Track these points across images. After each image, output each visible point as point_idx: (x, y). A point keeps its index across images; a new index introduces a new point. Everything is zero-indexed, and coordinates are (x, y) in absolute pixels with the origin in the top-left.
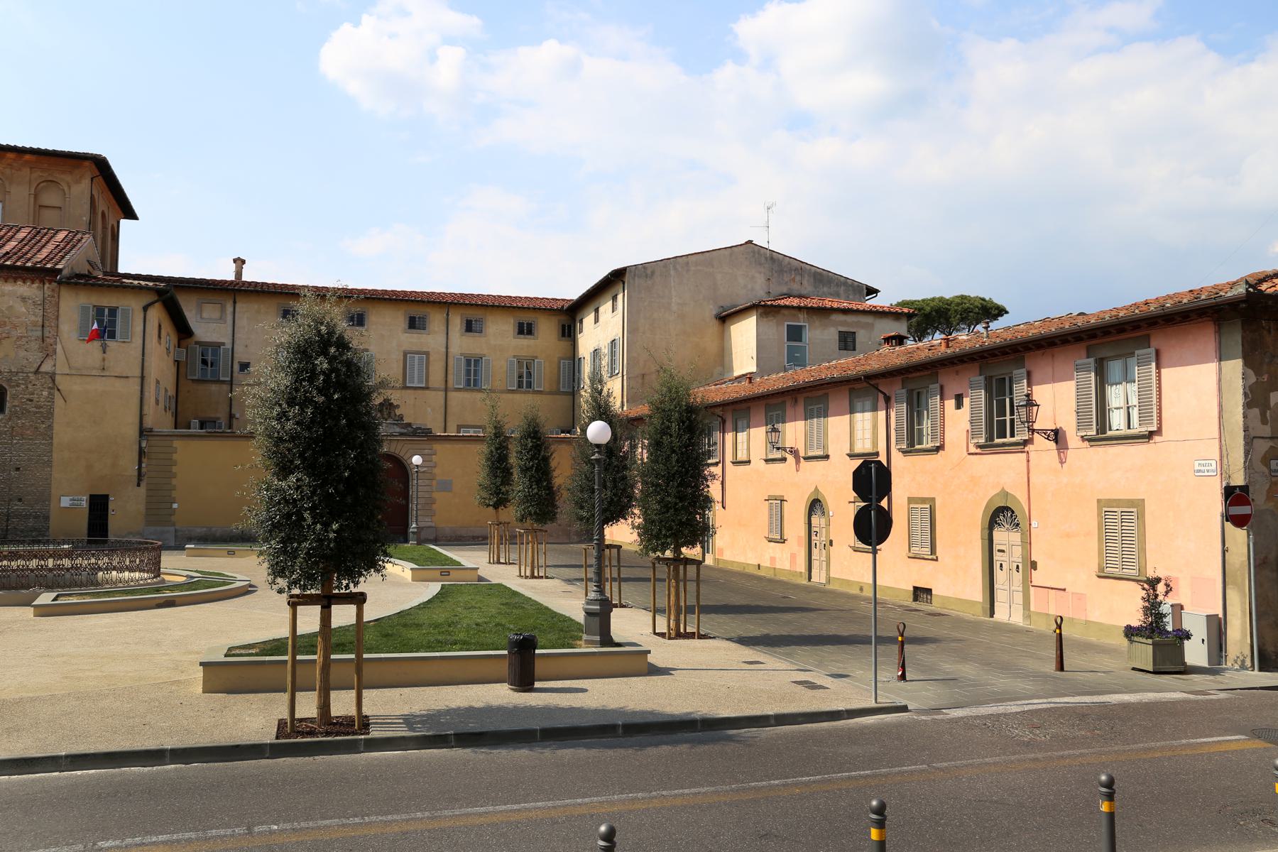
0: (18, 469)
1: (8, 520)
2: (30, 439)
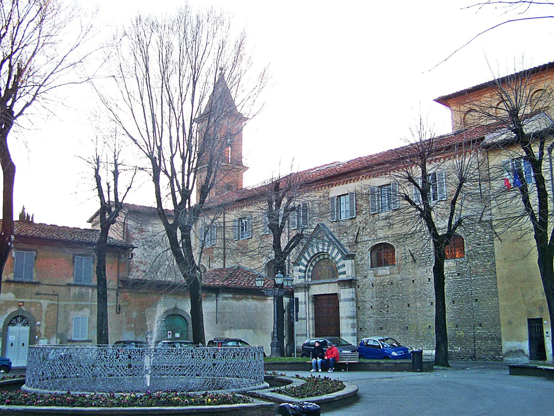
0: (477, 300)
1: (474, 341)
2: (482, 276)
